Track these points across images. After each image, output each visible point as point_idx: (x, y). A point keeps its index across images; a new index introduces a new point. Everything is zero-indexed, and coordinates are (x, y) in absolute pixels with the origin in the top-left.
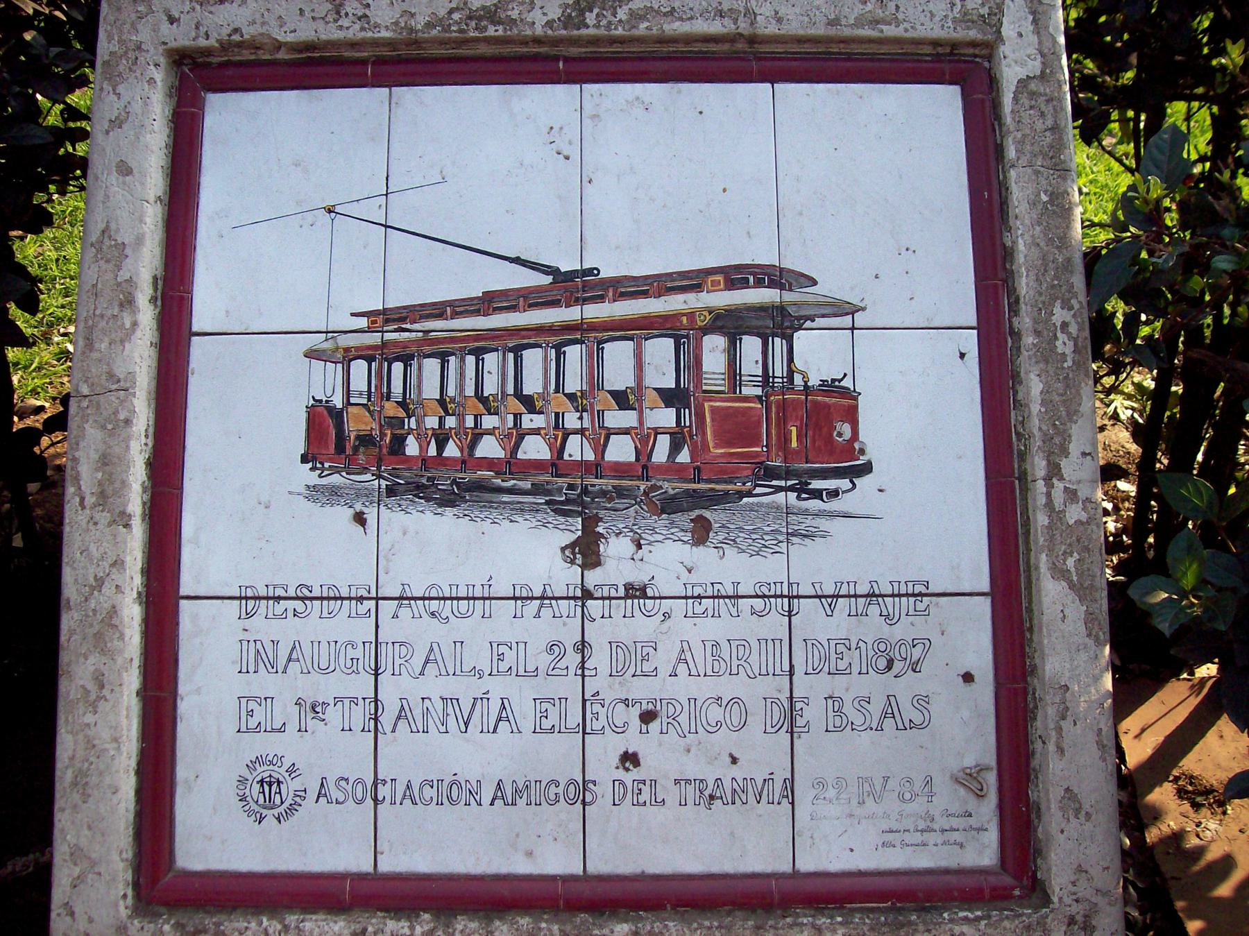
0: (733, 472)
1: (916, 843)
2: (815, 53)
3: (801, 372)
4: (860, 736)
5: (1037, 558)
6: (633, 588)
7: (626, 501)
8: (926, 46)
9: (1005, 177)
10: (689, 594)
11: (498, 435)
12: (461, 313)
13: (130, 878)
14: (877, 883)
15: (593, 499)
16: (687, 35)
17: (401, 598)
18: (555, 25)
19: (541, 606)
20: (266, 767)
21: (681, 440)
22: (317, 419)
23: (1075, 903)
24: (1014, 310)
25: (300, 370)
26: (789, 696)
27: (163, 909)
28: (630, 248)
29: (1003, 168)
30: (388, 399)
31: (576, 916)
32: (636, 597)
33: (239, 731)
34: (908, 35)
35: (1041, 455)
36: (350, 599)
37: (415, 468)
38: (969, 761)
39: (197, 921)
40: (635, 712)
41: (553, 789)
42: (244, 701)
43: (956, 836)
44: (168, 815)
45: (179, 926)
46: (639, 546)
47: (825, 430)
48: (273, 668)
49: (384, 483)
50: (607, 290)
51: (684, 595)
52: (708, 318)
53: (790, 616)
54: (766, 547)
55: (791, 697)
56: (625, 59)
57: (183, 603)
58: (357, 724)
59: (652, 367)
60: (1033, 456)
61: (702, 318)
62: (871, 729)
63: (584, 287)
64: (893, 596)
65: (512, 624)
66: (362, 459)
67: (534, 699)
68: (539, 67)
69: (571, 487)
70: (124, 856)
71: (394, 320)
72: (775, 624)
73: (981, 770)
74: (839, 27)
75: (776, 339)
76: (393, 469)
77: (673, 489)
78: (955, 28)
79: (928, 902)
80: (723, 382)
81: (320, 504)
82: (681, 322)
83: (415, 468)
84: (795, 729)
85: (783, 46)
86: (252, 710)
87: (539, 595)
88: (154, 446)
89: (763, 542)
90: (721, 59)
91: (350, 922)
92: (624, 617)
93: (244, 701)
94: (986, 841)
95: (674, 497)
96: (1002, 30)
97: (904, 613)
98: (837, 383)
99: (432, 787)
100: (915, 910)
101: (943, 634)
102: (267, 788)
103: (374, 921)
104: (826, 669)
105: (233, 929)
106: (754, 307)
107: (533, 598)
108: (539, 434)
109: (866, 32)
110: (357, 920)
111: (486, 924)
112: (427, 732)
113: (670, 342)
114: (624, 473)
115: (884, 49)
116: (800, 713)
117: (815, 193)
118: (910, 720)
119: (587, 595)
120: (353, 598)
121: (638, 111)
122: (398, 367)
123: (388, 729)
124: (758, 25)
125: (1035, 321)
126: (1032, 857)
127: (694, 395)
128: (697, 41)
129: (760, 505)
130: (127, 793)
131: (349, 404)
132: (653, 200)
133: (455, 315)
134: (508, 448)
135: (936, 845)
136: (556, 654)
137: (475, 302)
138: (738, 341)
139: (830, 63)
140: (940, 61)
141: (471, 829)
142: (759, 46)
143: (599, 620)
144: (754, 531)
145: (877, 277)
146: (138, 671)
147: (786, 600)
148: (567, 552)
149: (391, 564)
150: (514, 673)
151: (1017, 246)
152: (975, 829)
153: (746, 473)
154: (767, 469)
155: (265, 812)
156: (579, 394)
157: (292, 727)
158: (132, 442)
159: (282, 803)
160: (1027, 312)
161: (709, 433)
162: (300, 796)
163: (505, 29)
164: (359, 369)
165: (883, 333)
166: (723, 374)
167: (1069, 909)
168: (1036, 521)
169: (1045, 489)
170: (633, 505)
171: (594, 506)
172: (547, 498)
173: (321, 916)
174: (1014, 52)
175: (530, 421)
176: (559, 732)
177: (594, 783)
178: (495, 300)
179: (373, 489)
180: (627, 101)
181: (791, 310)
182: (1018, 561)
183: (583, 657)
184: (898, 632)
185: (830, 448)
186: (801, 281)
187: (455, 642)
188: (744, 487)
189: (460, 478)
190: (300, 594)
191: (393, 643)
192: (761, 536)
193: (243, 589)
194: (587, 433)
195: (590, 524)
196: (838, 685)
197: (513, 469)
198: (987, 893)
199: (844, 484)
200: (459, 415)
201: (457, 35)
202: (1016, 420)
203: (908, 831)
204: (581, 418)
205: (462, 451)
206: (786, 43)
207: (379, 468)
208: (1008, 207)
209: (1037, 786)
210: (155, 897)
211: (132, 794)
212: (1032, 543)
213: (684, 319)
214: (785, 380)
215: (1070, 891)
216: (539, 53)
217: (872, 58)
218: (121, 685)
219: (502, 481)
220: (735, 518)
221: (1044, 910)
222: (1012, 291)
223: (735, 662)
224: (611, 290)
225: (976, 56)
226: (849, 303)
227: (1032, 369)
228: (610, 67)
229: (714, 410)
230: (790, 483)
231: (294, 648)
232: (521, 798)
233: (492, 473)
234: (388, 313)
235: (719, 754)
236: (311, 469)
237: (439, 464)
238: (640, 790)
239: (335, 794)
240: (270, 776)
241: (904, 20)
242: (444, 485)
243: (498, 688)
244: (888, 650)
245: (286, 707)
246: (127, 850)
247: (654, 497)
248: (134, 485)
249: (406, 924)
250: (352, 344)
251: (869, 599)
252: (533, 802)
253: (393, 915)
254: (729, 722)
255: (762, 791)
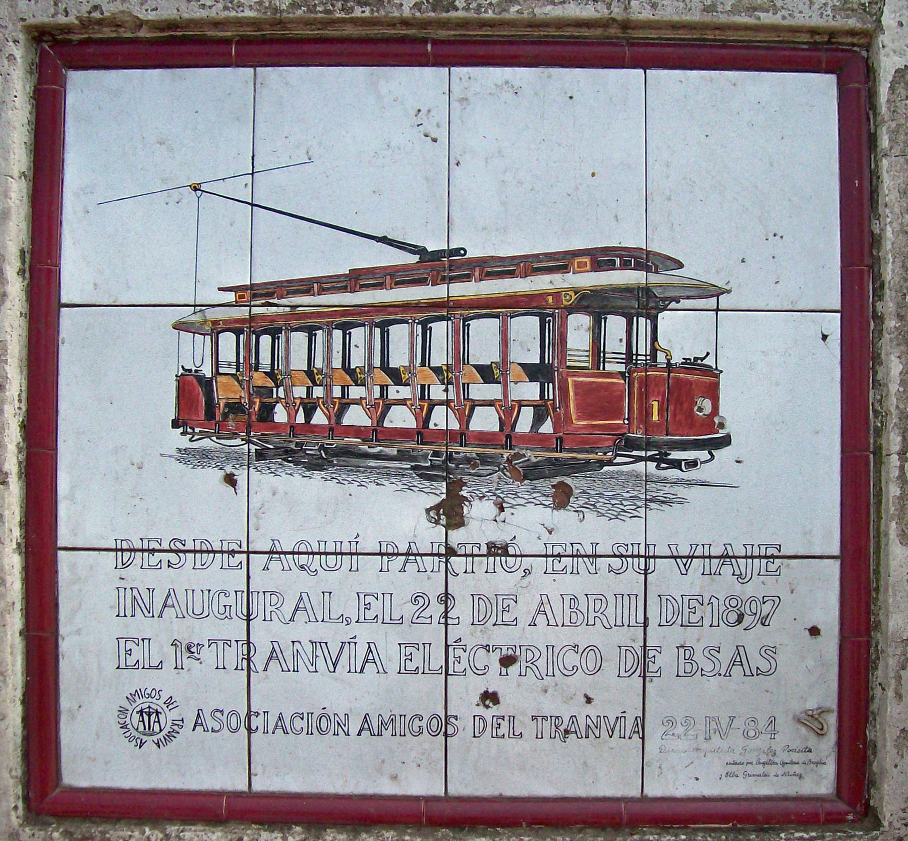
0: (595, 443)
1: (758, 774)
2: (689, 39)
3: (664, 351)
4: (708, 681)
5: (887, 526)
6: (495, 547)
7: (489, 467)
8: (803, 34)
9: (877, 166)
10: (550, 552)
11: (365, 405)
12: (328, 289)
13: (20, 793)
14: (720, 807)
15: (457, 466)
16: (559, 19)
17: (271, 552)
18: (424, 7)
19: (406, 562)
20: (145, 700)
21: (545, 412)
22: (186, 388)
23: (904, 826)
24: (879, 294)
25: (169, 341)
26: (642, 645)
27: (51, 819)
28: (497, 230)
29: (875, 157)
30: (257, 369)
31: (437, 831)
32: (498, 555)
33: (118, 668)
34: (786, 23)
35: (897, 431)
36: (222, 552)
37: (284, 434)
38: (812, 704)
39: (84, 830)
40: (496, 657)
41: (417, 723)
42: (122, 642)
43: (796, 768)
44: (53, 739)
45: (66, 833)
46: (502, 509)
47: (686, 405)
48: (149, 613)
49: (253, 448)
50: (473, 269)
51: (544, 553)
52: (574, 298)
53: (646, 574)
54: (625, 511)
55: (645, 646)
56: (495, 43)
57: (61, 554)
58: (231, 663)
59: (517, 344)
60: (888, 432)
61: (568, 297)
62: (720, 675)
63: (450, 266)
64: (746, 557)
65: (378, 577)
66: (231, 425)
67: (400, 644)
68: (407, 49)
69: (436, 454)
70: (14, 773)
71: (262, 296)
72: (632, 581)
73: (823, 712)
74: (715, 14)
75: (640, 319)
76: (262, 435)
77: (536, 457)
78: (834, 17)
79: (767, 823)
80: (587, 359)
81: (192, 466)
82: (547, 301)
83: (284, 434)
84: (647, 674)
85: (657, 31)
86: (130, 650)
87: (405, 552)
88: (27, 410)
89: (622, 507)
90: (592, 44)
91: (227, 832)
92: (486, 572)
93: (122, 642)
94: (824, 773)
95: (536, 465)
96: (883, 19)
97: (755, 572)
98: (699, 361)
99: (302, 719)
100: (754, 831)
101: (792, 592)
102: (146, 718)
103: (249, 832)
104: (679, 622)
105: (118, 837)
106: (620, 288)
107: (398, 554)
108: (405, 405)
109: (743, 19)
110: (233, 831)
111: (353, 836)
112: (298, 671)
113: (536, 320)
114: (489, 442)
115: (761, 37)
116: (653, 660)
117: (684, 179)
118: (757, 668)
119: (451, 552)
120: (225, 552)
121: (508, 95)
122: (266, 340)
123: (260, 668)
124: (632, 11)
125: (899, 306)
126: (866, 788)
127: (558, 371)
128: (569, 25)
129: (621, 473)
130: (14, 720)
131: (218, 373)
132: (520, 183)
133: (322, 291)
134: (374, 417)
135: (776, 776)
136: (421, 604)
137: (342, 279)
138: (603, 321)
139: (704, 50)
140: (816, 50)
141: (340, 756)
142: (633, 32)
143: (462, 575)
144: (613, 497)
145: (743, 261)
146: (20, 613)
147: (642, 560)
148: (432, 514)
149: (261, 521)
150: (380, 621)
151: (885, 233)
152: (813, 763)
153: (607, 444)
154: (628, 440)
155: (145, 738)
156: (445, 368)
157: (169, 664)
158: (5, 406)
159: (161, 730)
160: (891, 297)
161: (572, 406)
162: (178, 725)
163: (372, 10)
164: (228, 340)
165: (747, 315)
166: (587, 351)
167: (898, 832)
168: (889, 492)
169: (899, 463)
170: (497, 472)
171: (458, 471)
172: (413, 464)
173: (199, 827)
174: (893, 41)
175: (395, 392)
176: (423, 673)
177: (456, 718)
178: (361, 278)
179: (243, 453)
180: (496, 85)
181: (657, 292)
182: (869, 529)
183: (446, 608)
184: (749, 590)
185: (690, 422)
186: (668, 264)
187: (323, 592)
188: (605, 457)
189: (327, 444)
190: (173, 547)
191: (264, 592)
192: (621, 501)
193: (119, 542)
194: (452, 404)
195: (454, 488)
196: (690, 636)
197: (380, 437)
198: (822, 817)
199: (703, 455)
200: (326, 385)
201: (323, 15)
202: (874, 399)
203: (751, 763)
204: (446, 390)
205: (329, 419)
206: (660, 28)
207: (248, 433)
208: (878, 196)
209: (875, 726)
210: (44, 808)
211: (19, 721)
212: (883, 511)
213: (550, 299)
214: (648, 358)
215: (900, 817)
216: (408, 35)
217: (747, 45)
218: (4, 626)
219: (369, 447)
220: (595, 484)
221: (875, 832)
222: (877, 277)
223: (592, 615)
224: (477, 270)
225: (854, 45)
226: (714, 286)
227: (893, 351)
228: (480, 50)
229: (577, 385)
230: (649, 453)
231: (169, 595)
232: (386, 730)
233: (359, 440)
234: (256, 288)
235: (574, 695)
236: (181, 433)
237: (307, 431)
238: (499, 724)
239: (211, 723)
240: (149, 707)
241: (783, 8)
242: (312, 450)
243: (364, 634)
244: (739, 605)
245: (163, 646)
246: (16, 769)
247: (516, 464)
248: (9, 446)
249: (279, 835)
250: (220, 317)
251: (722, 560)
252: (398, 734)
253: (266, 827)
254: (584, 667)
255: (614, 727)
